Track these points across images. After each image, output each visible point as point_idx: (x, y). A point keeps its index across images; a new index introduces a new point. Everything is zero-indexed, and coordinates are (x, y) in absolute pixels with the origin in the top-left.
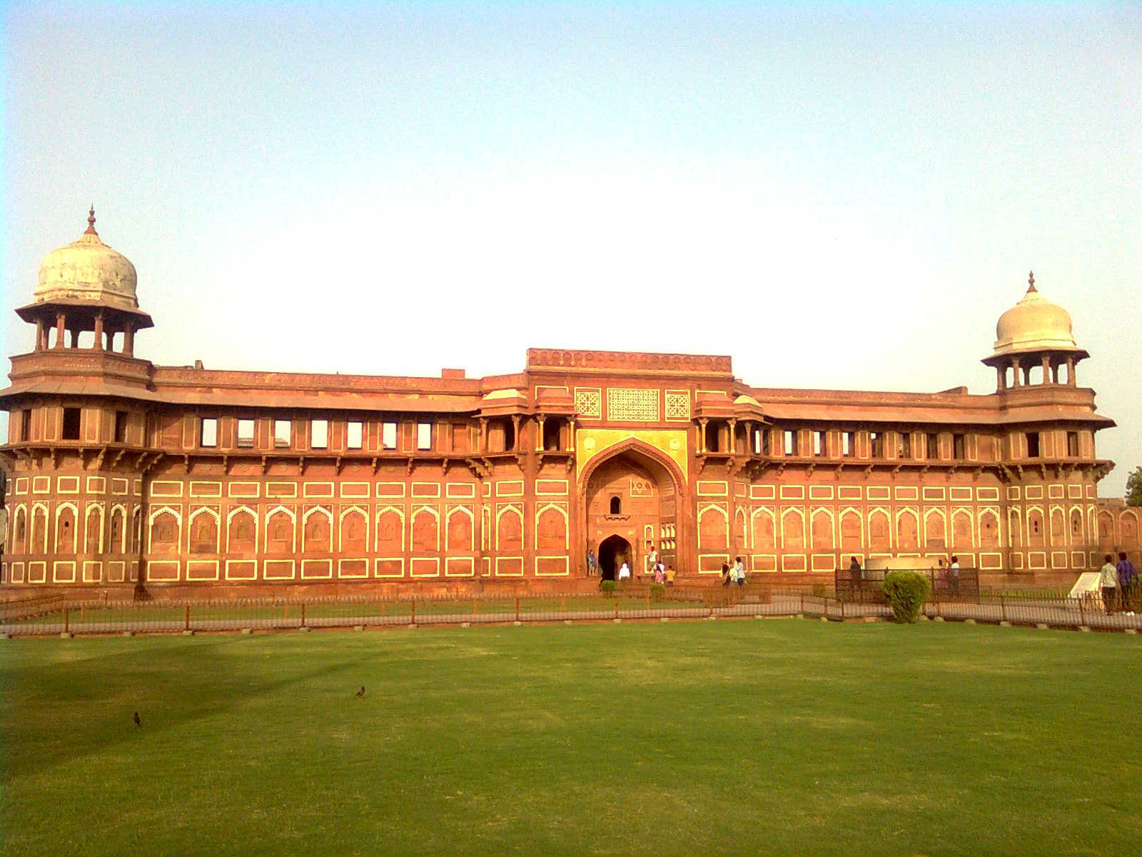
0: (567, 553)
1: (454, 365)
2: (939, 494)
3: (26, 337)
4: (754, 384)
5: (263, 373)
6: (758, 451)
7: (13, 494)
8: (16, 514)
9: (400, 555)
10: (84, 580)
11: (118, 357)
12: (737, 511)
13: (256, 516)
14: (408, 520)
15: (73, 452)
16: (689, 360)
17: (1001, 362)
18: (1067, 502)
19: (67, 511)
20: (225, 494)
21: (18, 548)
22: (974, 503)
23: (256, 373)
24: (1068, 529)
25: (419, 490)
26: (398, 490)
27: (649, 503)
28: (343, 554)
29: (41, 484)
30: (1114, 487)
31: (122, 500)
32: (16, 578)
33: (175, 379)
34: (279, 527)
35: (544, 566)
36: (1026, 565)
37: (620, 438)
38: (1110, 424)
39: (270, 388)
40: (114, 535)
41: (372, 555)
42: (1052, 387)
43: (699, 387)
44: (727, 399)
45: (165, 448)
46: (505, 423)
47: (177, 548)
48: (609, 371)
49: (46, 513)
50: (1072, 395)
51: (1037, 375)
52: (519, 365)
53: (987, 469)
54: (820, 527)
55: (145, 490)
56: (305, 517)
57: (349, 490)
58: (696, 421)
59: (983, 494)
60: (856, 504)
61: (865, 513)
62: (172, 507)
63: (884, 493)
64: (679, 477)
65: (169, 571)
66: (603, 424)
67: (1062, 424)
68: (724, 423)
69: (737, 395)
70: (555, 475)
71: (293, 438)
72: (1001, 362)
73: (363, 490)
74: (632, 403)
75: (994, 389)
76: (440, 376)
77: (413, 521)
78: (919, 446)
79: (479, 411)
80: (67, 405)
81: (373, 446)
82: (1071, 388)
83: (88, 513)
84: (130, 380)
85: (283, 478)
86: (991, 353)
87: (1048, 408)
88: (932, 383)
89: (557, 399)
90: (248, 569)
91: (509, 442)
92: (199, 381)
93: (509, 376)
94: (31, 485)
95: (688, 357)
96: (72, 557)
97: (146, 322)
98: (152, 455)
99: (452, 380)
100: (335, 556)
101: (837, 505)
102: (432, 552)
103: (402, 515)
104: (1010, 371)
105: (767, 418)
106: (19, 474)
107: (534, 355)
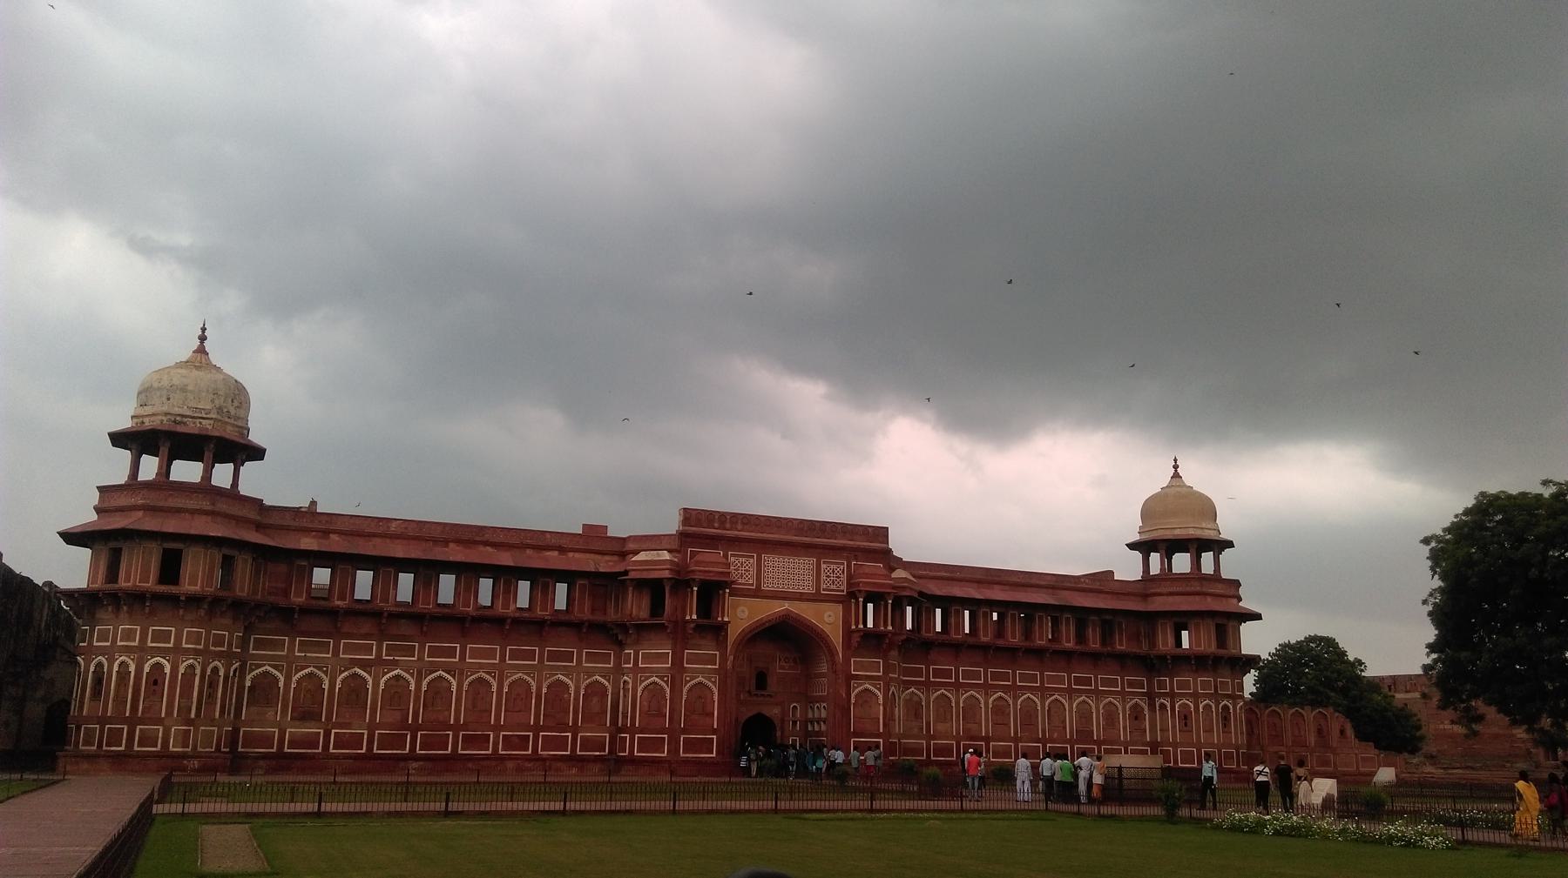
0: (714, 732)
2: (1087, 682)
3: (116, 466)
6: (870, 624)
7: (91, 643)
8: (92, 669)
9: (528, 728)
11: (219, 491)
15: (173, 600)
17: (1144, 547)
18: (1216, 697)
19: (158, 667)
20: (336, 653)
22: (1122, 693)
25: (554, 656)
28: (465, 727)
29: (129, 635)
31: (219, 656)
32: (86, 743)
33: (288, 521)
35: (691, 745)
36: (1176, 762)
38: (1258, 617)
40: (209, 696)
41: (497, 728)
44: (885, 572)
46: (654, 588)
48: (765, 536)
49: (132, 668)
55: (244, 643)
56: (425, 683)
58: (852, 595)
59: (1131, 684)
60: (1005, 689)
61: (1015, 698)
62: (275, 667)
63: (1033, 679)
64: (832, 652)
65: (266, 740)
66: (757, 593)
67: (1212, 614)
69: (893, 569)
72: (1144, 547)
74: (789, 573)
77: (544, 690)
79: (626, 573)
80: (166, 545)
82: (1216, 577)
83: (182, 670)
86: (1136, 537)
87: (1197, 598)
90: (356, 741)
92: (316, 525)
96: (159, 721)
97: (257, 453)
98: (258, 606)
99: (594, 537)
100: (456, 728)
101: (987, 688)
102: (565, 728)
104: (1155, 558)
105: (921, 594)
107: (689, 516)
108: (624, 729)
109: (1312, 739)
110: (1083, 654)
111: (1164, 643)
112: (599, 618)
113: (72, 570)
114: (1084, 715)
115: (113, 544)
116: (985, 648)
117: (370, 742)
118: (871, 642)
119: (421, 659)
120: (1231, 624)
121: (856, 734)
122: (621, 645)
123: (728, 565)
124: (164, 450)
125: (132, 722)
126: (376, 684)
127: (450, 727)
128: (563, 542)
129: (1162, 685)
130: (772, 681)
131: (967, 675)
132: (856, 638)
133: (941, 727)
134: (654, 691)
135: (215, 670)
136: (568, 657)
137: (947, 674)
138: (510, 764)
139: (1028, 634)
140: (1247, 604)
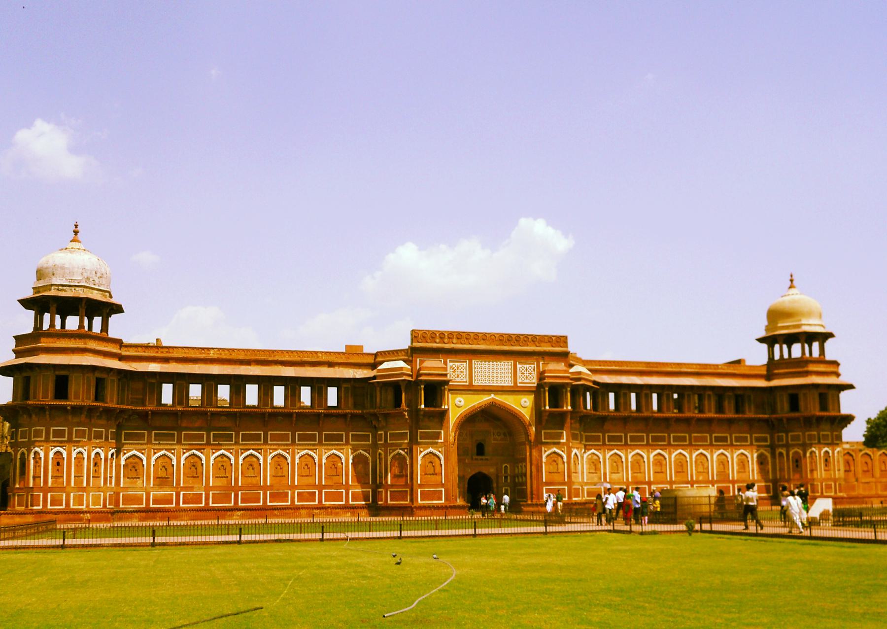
0: (443, 485)
1: (355, 343)
4: (584, 358)
5: (208, 349)
8: (19, 457)
9: (314, 486)
10: (72, 507)
12: (573, 454)
14: (320, 460)
15: (63, 408)
23: (203, 349)
29: (38, 434)
30: (854, 433)
32: (19, 505)
37: (485, 399)
38: (851, 387)
41: (293, 487)
43: (543, 359)
44: (565, 368)
46: (396, 388)
49: (42, 455)
50: (822, 366)
52: (405, 343)
53: (760, 420)
58: (540, 386)
61: (670, 454)
66: (470, 389)
68: (564, 386)
69: (571, 366)
74: (494, 373)
75: (765, 360)
76: (344, 351)
77: (324, 461)
78: (710, 404)
79: (374, 377)
81: (293, 404)
83: (74, 455)
94: (30, 433)
96: (62, 489)
99: (352, 356)
100: (265, 488)
105: (595, 382)
108: (381, 485)
110: (720, 420)
114: (723, 463)
116: (646, 419)
117: (207, 499)
120: (831, 393)
121: (547, 484)
122: (376, 429)
123: (446, 369)
125: (46, 490)
127: (260, 488)
129: (780, 439)
130: (488, 449)
132: (545, 418)
133: (615, 476)
138: (303, 512)
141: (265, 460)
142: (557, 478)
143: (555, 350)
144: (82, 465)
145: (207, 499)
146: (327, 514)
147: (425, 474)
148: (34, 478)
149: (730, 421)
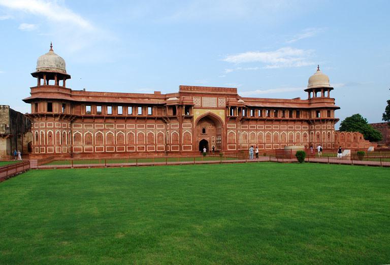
0: (191, 144)
3: (34, 82)
5: (103, 93)
13: (103, 134)
14: (146, 135)
15: (51, 116)
16: (225, 89)
18: (327, 130)
20: (94, 128)
21: (37, 143)
22: (302, 131)
24: (326, 136)
25: (149, 126)
26: (143, 126)
27: (213, 130)
28: (128, 145)
29: (42, 125)
31: (65, 129)
34: (110, 137)
35: (185, 148)
37: (206, 112)
38: (339, 108)
39: (105, 97)
40: (64, 139)
41: (136, 145)
42: (323, 98)
43: (228, 97)
45: (77, 114)
46: (173, 107)
47: (81, 143)
48: (203, 92)
49: (44, 133)
51: (319, 94)
52: (177, 91)
53: (305, 121)
54: (260, 137)
57: (129, 126)
58: (227, 107)
59: (304, 128)
61: (272, 133)
65: (80, 149)
66: (201, 108)
67: (326, 108)
69: (238, 100)
70: (188, 122)
71: (112, 112)
72: (309, 91)
73: (133, 127)
79: (166, 104)
81: (135, 114)
82: (328, 98)
83: (56, 133)
84: (65, 94)
85: (110, 123)
86: (307, 88)
88: (291, 97)
89: (189, 100)
90: (101, 149)
91: (175, 113)
93: (174, 94)
95: (225, 88)
96: (52, 146)
97: (69, 77)
98: (73, 116)
99: (157, 95)
100: (126, 145)
101: (264, 130)
102: (153, 144)
103: (144, 134)
104: (312, 93)
105: (246, 106)
106: (35, 122)
107: (181, 88)
109: (352, 140)
111: (314, 116)
112: (160, 116)
113: (27, 109)
114: (291, 136)
115: (36, 102)
116: (264, 120)
117: (105, 149)
118: (233, 119)
119: (115, 128)
120: (331, 111)
124: (45, 77)
125: (46, 146)
126: (105, 135)
127: (124, 145)
128: (150, 97)
131: (259, 127)
133: (252, 141)
134: (175, 134)
135: (64, 132)
136: (153, 127)
137: (254, 127)
138: (140, 154)
139: (276, 116)
140: (336, 105)
141: (126, 135)
142: (232, 142)
143: (232, 93)
144: (59, 137)
145: (105, 149)
146: (149, 155)
147: (185, 139)
148: (41, 141)
149: (294, 121)
